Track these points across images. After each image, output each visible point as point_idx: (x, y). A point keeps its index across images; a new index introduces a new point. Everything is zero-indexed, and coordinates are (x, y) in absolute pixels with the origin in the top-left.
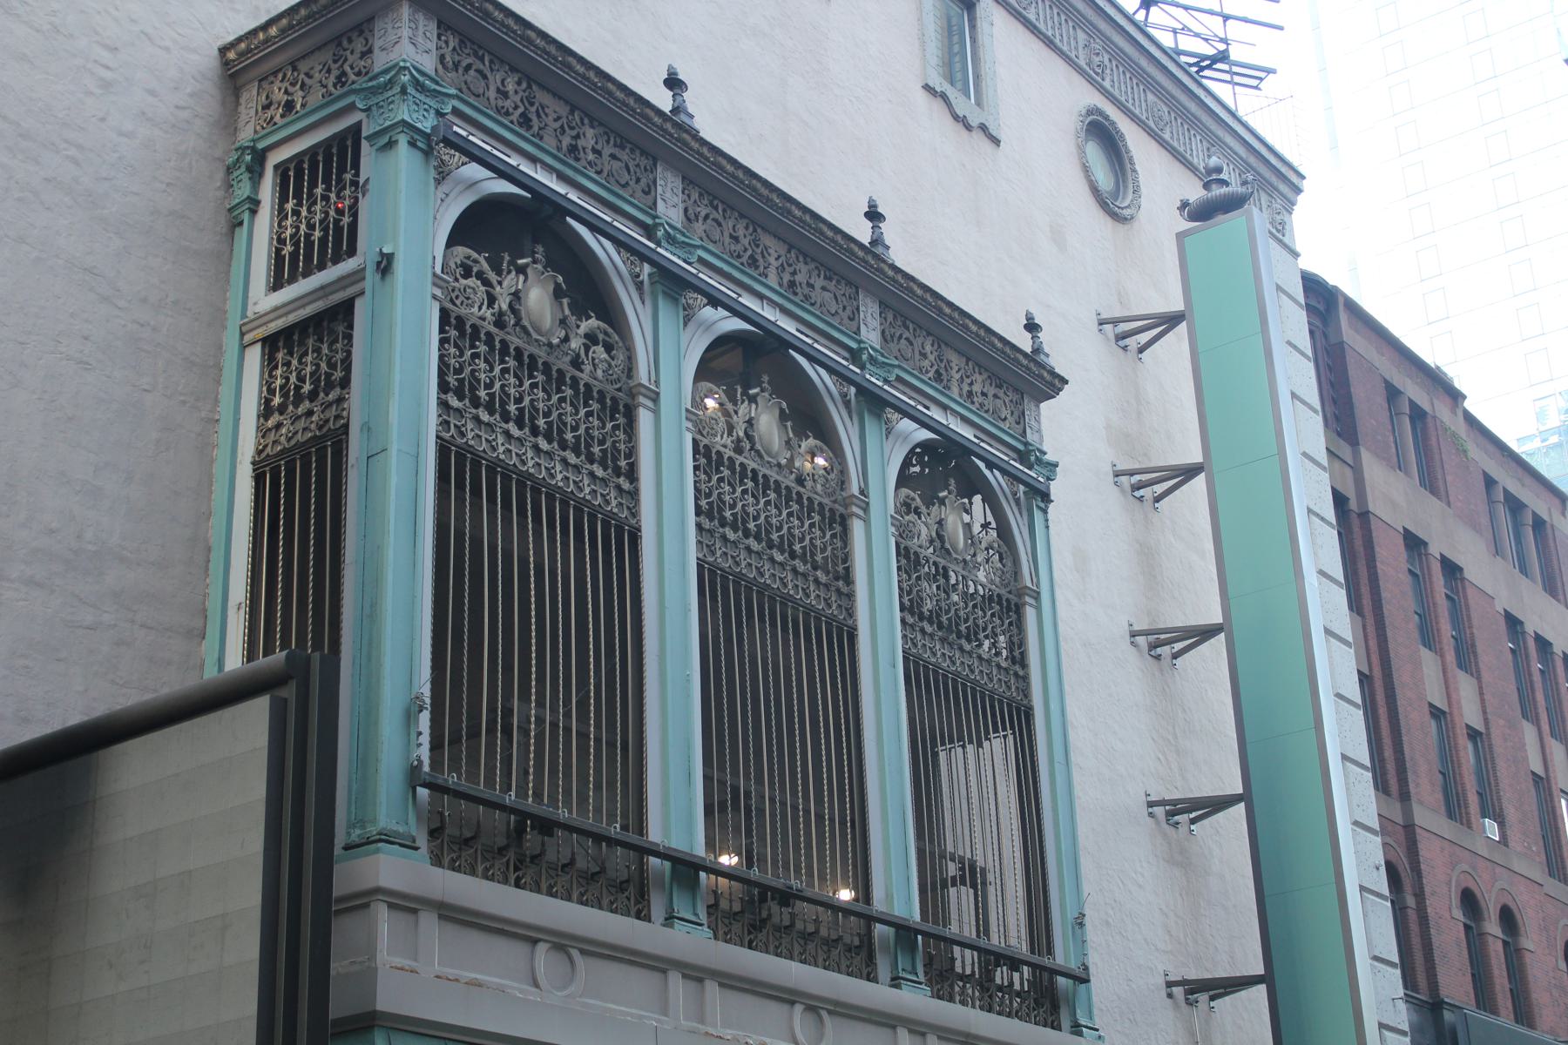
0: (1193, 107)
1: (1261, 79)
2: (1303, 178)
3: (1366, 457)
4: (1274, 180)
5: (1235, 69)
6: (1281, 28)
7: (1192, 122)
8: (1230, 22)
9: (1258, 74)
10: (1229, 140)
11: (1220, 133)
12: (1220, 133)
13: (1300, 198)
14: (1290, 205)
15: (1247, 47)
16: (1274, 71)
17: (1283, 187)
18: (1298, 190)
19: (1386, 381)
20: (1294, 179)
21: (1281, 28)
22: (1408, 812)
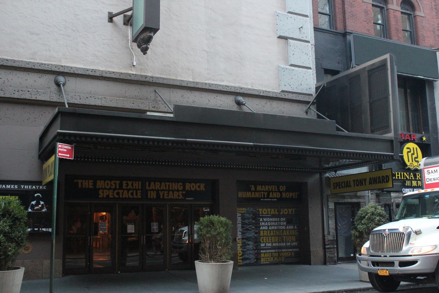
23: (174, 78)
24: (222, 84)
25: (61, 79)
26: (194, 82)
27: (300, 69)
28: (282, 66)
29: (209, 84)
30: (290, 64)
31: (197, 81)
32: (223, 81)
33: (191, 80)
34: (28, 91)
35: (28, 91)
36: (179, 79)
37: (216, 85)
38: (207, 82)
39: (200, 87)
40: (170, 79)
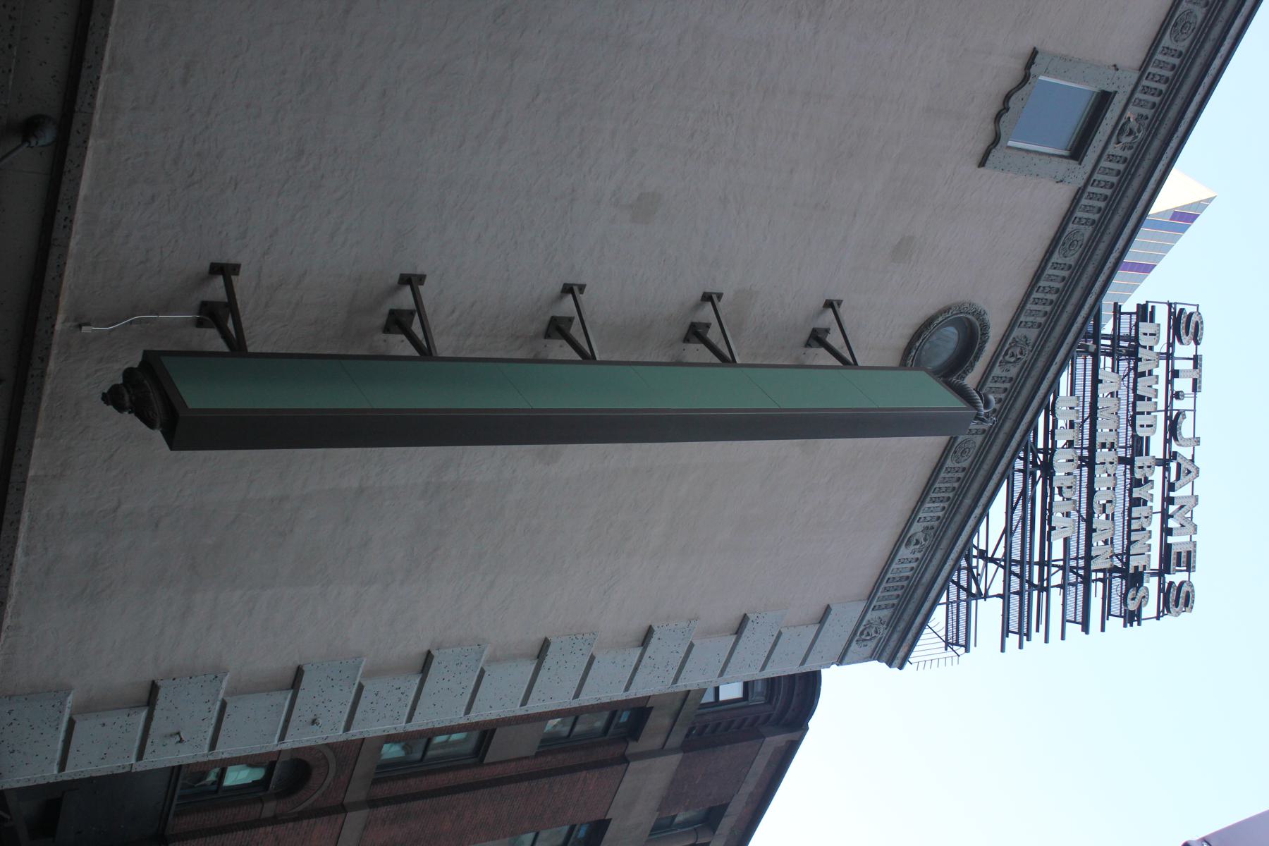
0: (967, 501)
1: (957, 644)
2: (901, 667)
3: (675, 759)
4: (902, 625)
5: (963, 605)
6: (1003, 650)
7: (953, 506)
8: (1000, 600)
9: (958, 639)
10: (939, 555)
11: (945, 543)
12: (945, 543)
13: (884, 665)
14: (876, 655)
15: (988, 613)
16: (967, 650)
17: (895, 637)
18: (890, 664)
19: (726, 806)
20: (901, 654)
21: (1003, 650)
22: (357, 806)
23: (40, 428)
24: (19, 552)
25: (48, 136)
26: (24, 482)
27: (60, 746)
28: (70, 698)
29: (19, 521)
30: (75, 717)
31: (30, 488)
32: (27, 554)
33: (31, 473)
34: (10, 46)
35: (10, 46)
36: (37, 441)
37: (16, 538)
38: (25, 515)
39: (9, 498)
40: (35, 421)
